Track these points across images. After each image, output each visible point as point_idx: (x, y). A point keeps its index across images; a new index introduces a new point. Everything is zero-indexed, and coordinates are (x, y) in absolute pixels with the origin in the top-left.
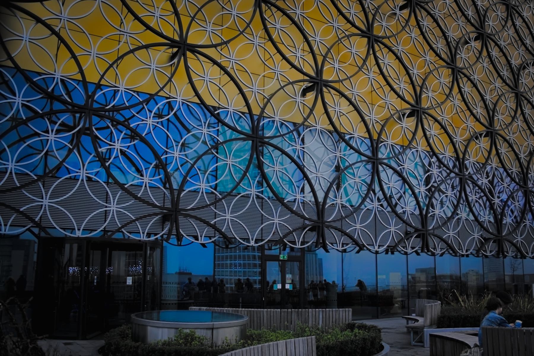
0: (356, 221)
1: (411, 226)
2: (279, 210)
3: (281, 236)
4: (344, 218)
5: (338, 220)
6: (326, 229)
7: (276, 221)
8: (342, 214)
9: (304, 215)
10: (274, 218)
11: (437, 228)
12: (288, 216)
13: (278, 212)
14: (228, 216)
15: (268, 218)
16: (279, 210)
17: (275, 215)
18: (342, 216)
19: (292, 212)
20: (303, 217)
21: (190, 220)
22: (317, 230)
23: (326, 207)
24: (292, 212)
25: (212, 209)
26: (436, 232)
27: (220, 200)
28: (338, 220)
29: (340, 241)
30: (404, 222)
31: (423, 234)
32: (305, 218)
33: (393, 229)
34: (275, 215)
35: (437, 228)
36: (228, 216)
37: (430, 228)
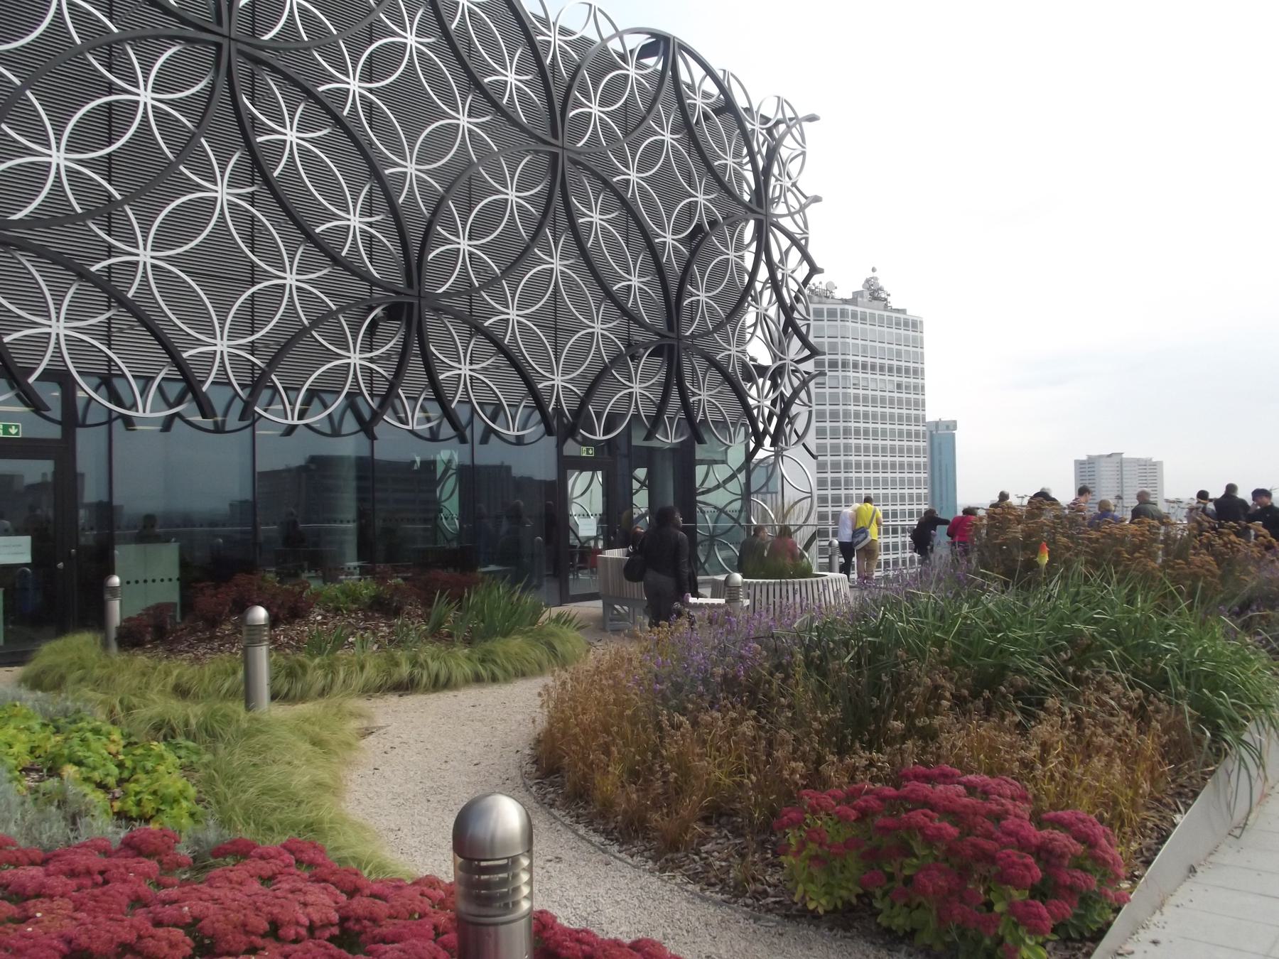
0: (507, 301)
1: (642, 324)
2: (299, 253)
3: (306, 322)
4: (478, 290)
5: (458, 294)
6: (429, 316)
7: (291, 279)
8: (470, 279)
9: (368, 271)
10: (285, 271)
11: (701, 336)
12: (325, 271)
13: (298, 257)
14: (291, 279)
15: (266, 271)
16: (299, 253)
17: (287, 264)
18: (471, 284)
19: (336, 260)
20: (365, 277)
21: (18, 254)
22: (404, 318)
23: (430, 257)
24: (336, 260)
25: (91, 230)
26: (701, 343)
27: (121, 203)
28: (458, 294)
29: (467, 347)
30: (625, 312)
31: (671, 347)
32: (373, 282)
33: (598, 328)
34: (287, 264)
35: (701, 336)
36: (145, 256)
37: (688, 334)
